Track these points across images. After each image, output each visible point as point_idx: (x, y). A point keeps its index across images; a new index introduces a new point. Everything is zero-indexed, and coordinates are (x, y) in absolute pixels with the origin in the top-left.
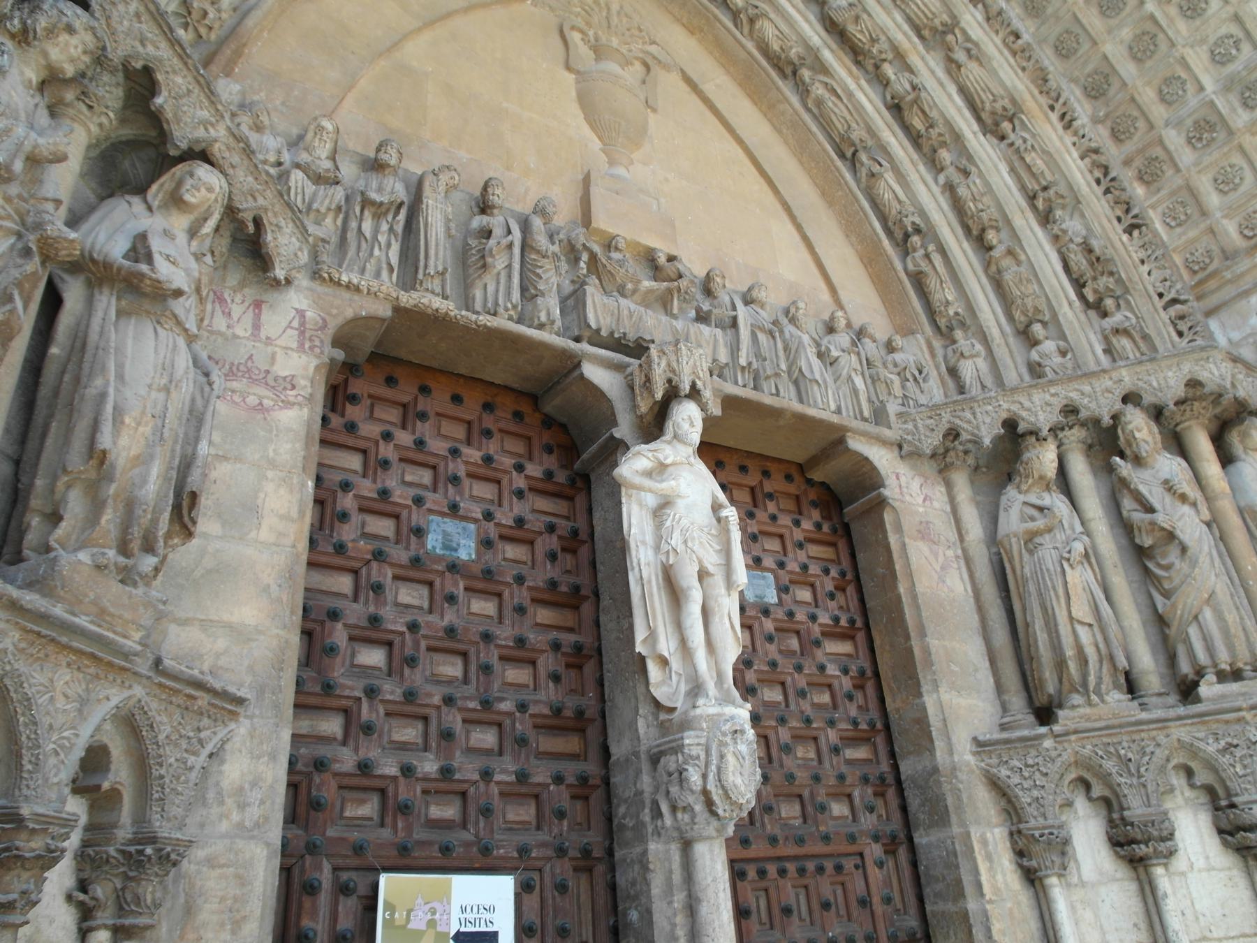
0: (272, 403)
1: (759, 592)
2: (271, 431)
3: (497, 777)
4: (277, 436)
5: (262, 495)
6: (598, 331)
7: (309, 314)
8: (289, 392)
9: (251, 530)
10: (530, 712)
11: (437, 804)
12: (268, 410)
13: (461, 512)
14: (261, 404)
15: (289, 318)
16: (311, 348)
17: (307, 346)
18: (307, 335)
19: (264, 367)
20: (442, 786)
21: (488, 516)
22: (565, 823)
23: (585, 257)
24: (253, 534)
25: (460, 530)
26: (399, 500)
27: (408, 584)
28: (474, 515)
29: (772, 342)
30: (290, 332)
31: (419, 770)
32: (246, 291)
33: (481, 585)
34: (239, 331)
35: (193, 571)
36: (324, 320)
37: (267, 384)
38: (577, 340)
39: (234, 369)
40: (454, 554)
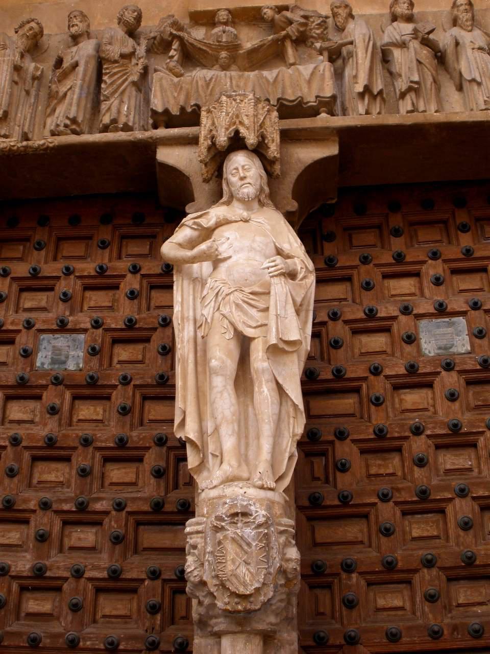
1: (443, 343)
3: (88, 574)
6: (166, 112)
10: (128, 509)
11: (36, 600)
13: (70, 326)
20: (36, 582)
21: (97, 324)
22: (159, 617)
23: (175, 45)
25: (70, 343)
26: (11, 328)
27: (88, 402)
28: (82, 326)
29: (365, 55)
31: (13, 569)
33: (87, 392)
38: (155, 127)
40: (63, 367)
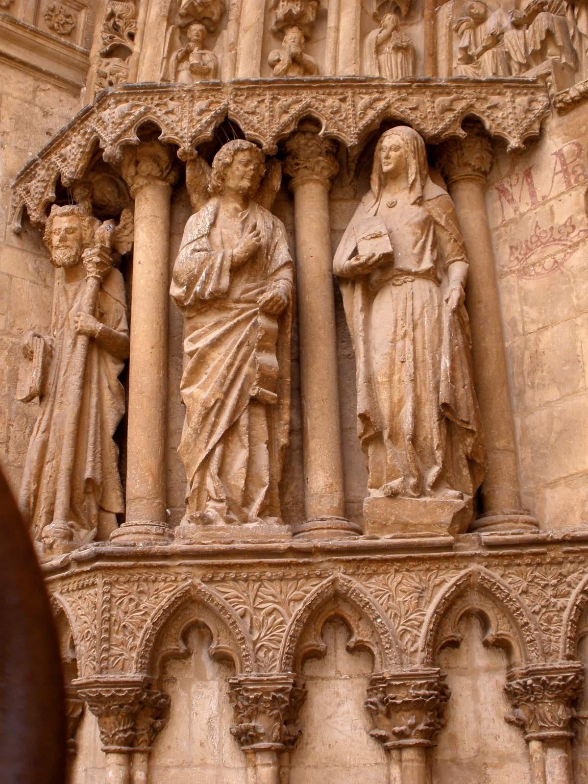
0: (562, 255)
2: (569, 281)
4: (575, 282)
5: (579, 344)
7: (565, 149)
8: (572, 235)
9: (579, 381)
12: (562, 264)
14: (556, 262)
15: (552, 166)
16: (576, 180)
17: (573, 181)
18: (570, 170)
19: (547, 228)
24: (581, 384)
30: (557, 178)
32: (517, 168)
34: (523, 209)
35: (549, 438)
36: (578, 145)
37: (555, 240)
39: (529, 244)
